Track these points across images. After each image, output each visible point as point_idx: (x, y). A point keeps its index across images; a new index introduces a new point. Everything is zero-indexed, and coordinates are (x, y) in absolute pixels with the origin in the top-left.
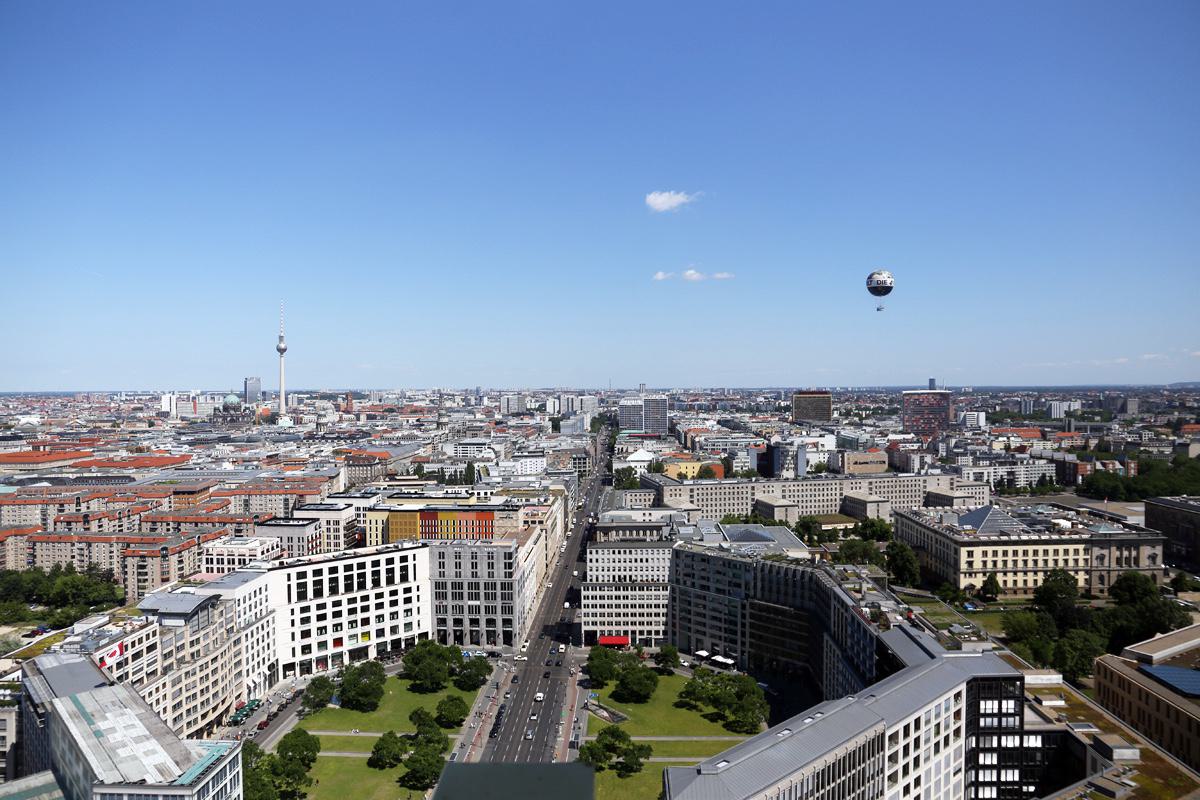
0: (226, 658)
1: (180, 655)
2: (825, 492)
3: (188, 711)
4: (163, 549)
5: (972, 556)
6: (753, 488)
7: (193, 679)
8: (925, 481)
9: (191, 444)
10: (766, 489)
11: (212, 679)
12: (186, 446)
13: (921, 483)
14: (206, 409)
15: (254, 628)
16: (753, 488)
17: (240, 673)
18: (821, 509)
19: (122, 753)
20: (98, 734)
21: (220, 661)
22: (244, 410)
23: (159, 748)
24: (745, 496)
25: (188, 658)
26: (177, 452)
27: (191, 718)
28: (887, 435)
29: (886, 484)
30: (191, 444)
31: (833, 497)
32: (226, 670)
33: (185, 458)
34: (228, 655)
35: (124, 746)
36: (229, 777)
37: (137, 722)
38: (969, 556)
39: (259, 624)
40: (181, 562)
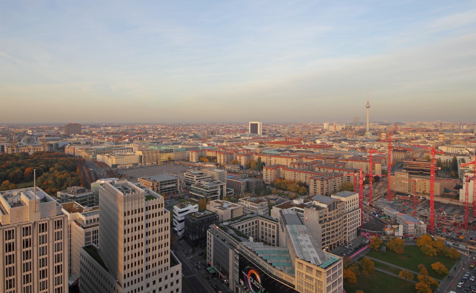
0: (341, 222)
1: (325, 218)
3: (327, 238)
4: (322, 178)
7: (329, 227)
9: (333, 141)
11: (335, 229)
14: (339, 128)
15: (352, 213)
17: (346, 229)
19: (304, 249)
20: (297, 240)
21: (339, 223)
23: (315, 252)
25: (328, 220)
26: (329, 143)
27: (328, 240)
30: (333, 141)
32: (341, 226)
33: (331, 146)
34: (342, 221)
35: (305, 247)
36: (338, 270)
37: (309, 240)
39: (354, 212)
40: (327, 183)
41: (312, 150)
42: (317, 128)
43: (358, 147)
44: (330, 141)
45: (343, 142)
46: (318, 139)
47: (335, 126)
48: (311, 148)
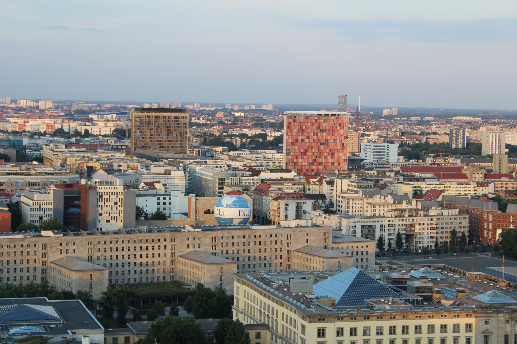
2: (150, 252)
5: (323, 336)
6: (44, 246)
8: (289, 237)
10: (64, 248)
13: (284, 239)
16: (44, 246)
18: (144, 276)
24: (32, 257)
28: (256, 173)
29: (236, 240)
31: (162, 259)
38: (319, 336)
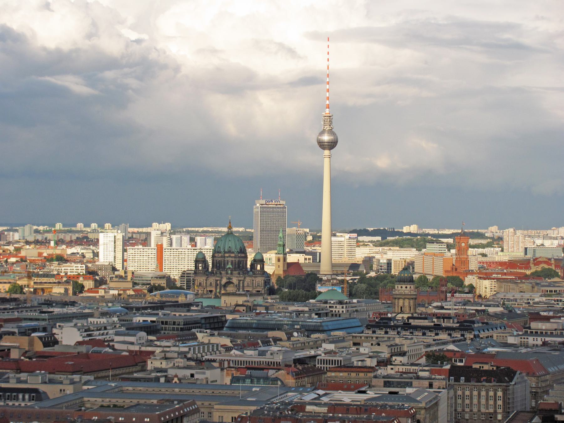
9: (150, 329)
12: (143, 334)
22: (252, 265)
26: (125, 344)
33: (138, 359)
41: (34, 381)
42: (61, 259)
43: (279, 358)
44: (132, 329)
45: (202, 336)
46: (67, 318)
47: (160, 249)
48: (31, 371)
